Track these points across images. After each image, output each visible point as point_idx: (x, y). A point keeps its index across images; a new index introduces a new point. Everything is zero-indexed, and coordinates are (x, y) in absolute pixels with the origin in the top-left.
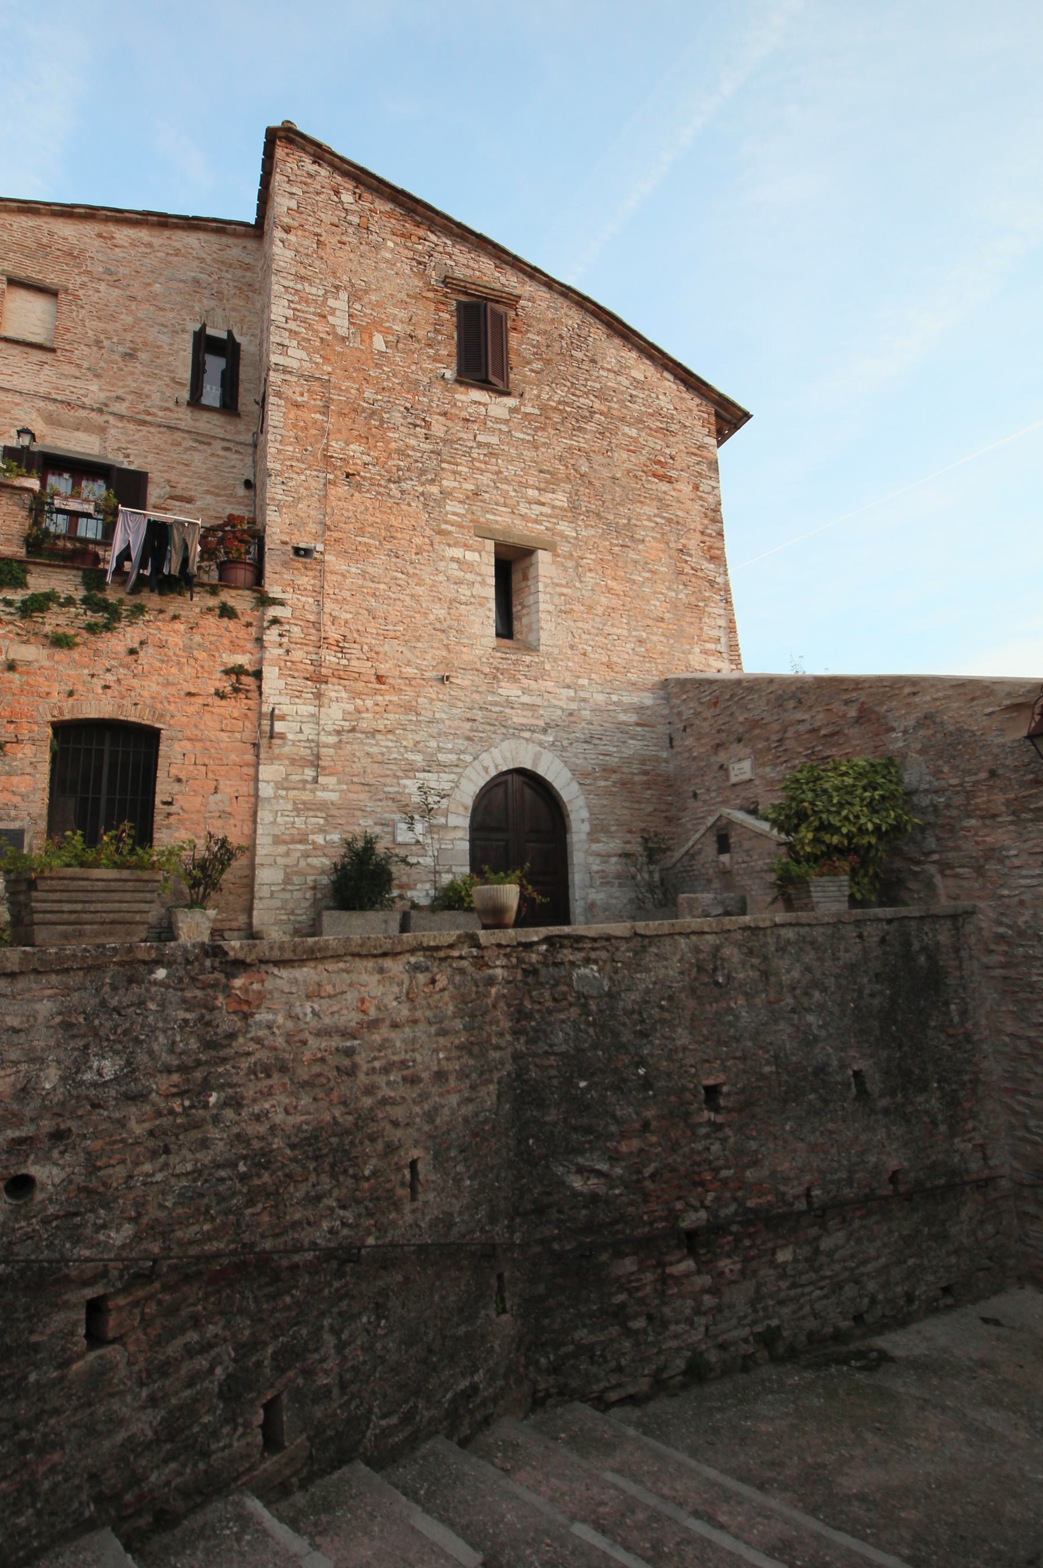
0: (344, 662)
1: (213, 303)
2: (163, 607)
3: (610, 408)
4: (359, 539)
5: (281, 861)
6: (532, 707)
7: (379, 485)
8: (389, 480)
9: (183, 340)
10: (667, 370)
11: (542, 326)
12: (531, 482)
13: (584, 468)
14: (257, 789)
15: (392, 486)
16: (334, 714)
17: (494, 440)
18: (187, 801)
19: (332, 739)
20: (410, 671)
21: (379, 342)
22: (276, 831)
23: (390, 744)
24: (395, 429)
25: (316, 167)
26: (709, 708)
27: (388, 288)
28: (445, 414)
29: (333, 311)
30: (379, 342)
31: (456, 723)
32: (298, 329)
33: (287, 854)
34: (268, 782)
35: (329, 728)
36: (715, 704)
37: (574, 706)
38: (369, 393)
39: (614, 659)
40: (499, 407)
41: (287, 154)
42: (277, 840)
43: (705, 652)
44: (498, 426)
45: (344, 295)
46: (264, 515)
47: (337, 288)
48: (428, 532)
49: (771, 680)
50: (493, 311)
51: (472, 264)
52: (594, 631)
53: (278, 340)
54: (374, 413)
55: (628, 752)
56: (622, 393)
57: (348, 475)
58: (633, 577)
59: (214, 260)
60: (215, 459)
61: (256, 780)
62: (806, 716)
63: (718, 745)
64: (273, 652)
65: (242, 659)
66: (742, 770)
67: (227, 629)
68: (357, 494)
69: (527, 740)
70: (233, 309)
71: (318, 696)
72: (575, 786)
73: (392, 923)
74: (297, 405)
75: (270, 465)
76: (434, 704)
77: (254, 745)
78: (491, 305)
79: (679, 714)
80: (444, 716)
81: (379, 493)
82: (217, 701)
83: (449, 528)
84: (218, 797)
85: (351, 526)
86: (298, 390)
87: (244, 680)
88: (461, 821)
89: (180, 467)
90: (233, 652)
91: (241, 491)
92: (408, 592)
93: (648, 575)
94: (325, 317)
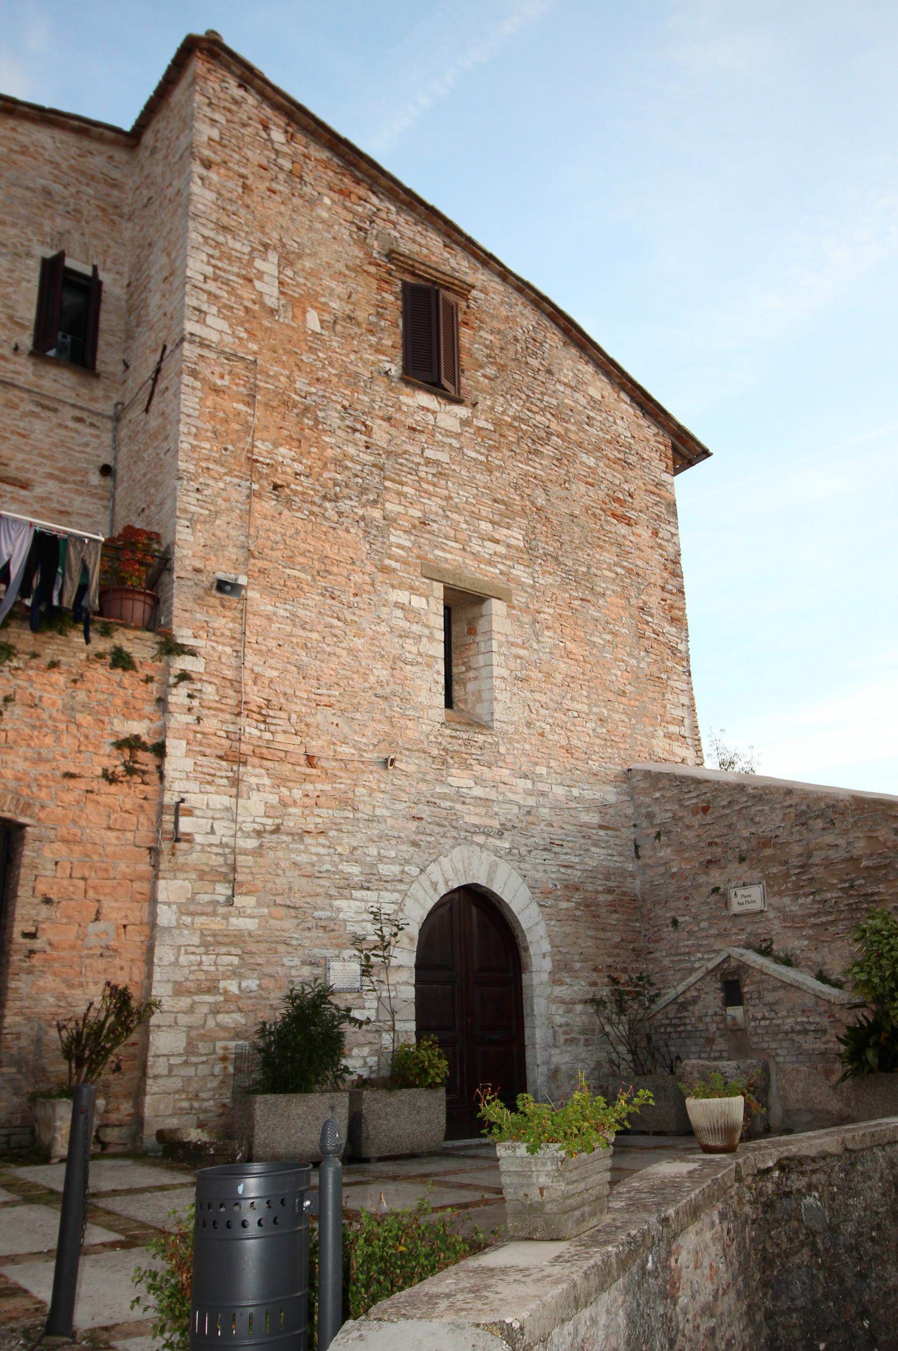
0: (268, 736)
1: (69, 224)
2: (38, 649)
3: (567, 430)
4: (288, 571)
5: (183, 1020)
6: (485, 801)
7: (313, 503)
8: (325, 497)
9: (28, 267)
10: (624, 390)
11: (495, 324)
12: (484, 513)
13: (541, 502)
14: (153, 914)
15: (328, 505)
16: (255, 807)
17: (443, 457)
18: (57, 932)
19: (251, 843)
20: (346, 750)
21: (313, 320)
22: (178, 976)
23: (323, 851)
24: (333, 432)
25: (241, 92)
27: (325, 255)
28: (389, 419)
29: (261, 275)
30: (313, 320)
31: (401, 822)
32: (218, 292)
33: (191, 1010)
34: (169, 904)
35: (248, 827)
36: (705, 810)
37: (531, 802)
38: (301, 384)
39: (575, 742)
40: (449, 417)
41: (209, 70)
42: (179, 990)
43: (668, 736)
44: (449, 440)
45: (273, 257)
46: (174, 532)
47: (266, 246)
48: (369, 568)
49: (788, 790)
50: (446, 302)
51: (418, 238)
52: (552, 705)
53: (194, 303)
54: (307, 409)
55: (591, 863)
56: (580, 413)
57: (276, 487)
58: (594, 639)
59: (71, 167)
60: (63, 432)
61: (153, 900)
62: (841, 841)
63: (709, 862)
64: (179, 720)
65: (138, 728)
66: (749, 897)
67: (120, 684)
68: (286, 512)
69: (481, 846)
70: (95, 236)
71: (236, 782)
72: (535, 909)
73: (339, 1110)
74: (216, 390)
75: (182, 465)
76: (376, 796)
77: (150, 849)
78: (443, 292)
79: (650, 816)
80: (386, 813)
81: (312, 513)
82: (105, 787)
83: (397, 565)
84: (101, 925)
85: (279, 553)
86: (218, 370)
87: (141, 757)
88: (405, 956)
89: (15, 438)
90: (127, 717)
91: (95, 479)
92: (344, 645)
93: (609, 637)
94: (250, 281)
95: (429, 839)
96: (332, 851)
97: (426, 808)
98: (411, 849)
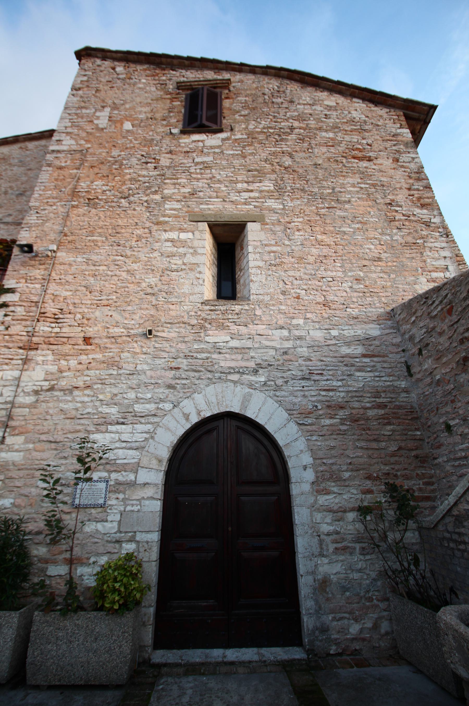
4: (89, 238)
6: (242, 350)
15: (123, 200)
23: (86, 399)
26: (443, 320)
35: (29, 389)
37: (288, 345)
44: (213, 150)
72: (293, 428)
76: (140, 359)
80: (146, 367)
81: (110, 207)
83: (167, 219)
92: (125, 269)
95: (184, 382)
96: (94, 398)
97: (185, 361)
98: (167, 391)
